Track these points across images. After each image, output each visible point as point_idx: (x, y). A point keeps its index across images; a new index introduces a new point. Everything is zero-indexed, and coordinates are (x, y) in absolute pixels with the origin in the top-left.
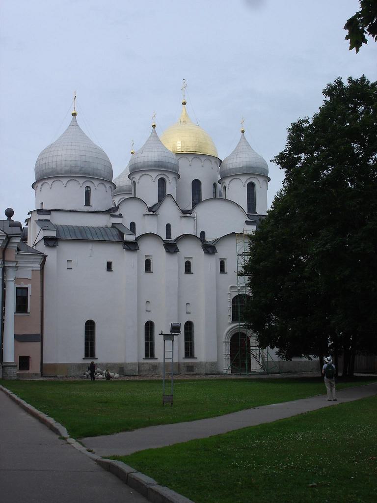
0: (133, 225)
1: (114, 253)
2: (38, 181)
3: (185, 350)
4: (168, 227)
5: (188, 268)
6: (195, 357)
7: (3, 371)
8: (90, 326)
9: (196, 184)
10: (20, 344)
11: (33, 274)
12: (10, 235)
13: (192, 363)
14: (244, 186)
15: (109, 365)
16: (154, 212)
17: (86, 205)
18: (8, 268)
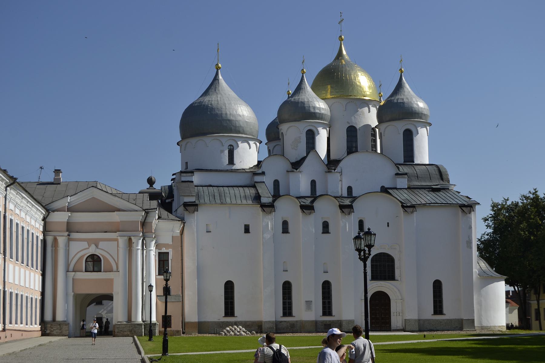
3: (323, 309)
6: (333, 315)
12: (147, 209)
13: (330, 321)
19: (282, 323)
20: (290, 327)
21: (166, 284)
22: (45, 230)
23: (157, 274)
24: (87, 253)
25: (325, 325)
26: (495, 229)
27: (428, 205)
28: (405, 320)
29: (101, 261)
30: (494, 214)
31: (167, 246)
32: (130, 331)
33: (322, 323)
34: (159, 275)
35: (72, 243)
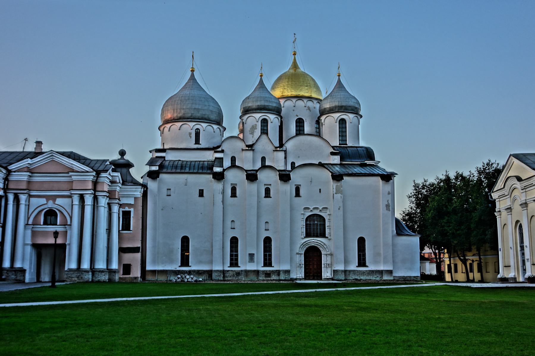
0: (233, 159)
2: (163, 124)
4: (263, 159)
5: (268, 192)
7: (93, 275)
9: (300, 123)
13: (270, 271)
14: (336, 122)
15: (200, 272)
16: (249, 148)
17: (195, 144)
18: (98, 197)
19: (229, 272)
20: (235, 276)
23: (121, 229)
25: (265, 274)
26: (417, 204)
27: (354, 174)
28: (334, 270)
30: (416, 192)
31: (130, 205)
32: (77, 277)
33: (263, 272)
34: (123, 230)
35: (32, 199)
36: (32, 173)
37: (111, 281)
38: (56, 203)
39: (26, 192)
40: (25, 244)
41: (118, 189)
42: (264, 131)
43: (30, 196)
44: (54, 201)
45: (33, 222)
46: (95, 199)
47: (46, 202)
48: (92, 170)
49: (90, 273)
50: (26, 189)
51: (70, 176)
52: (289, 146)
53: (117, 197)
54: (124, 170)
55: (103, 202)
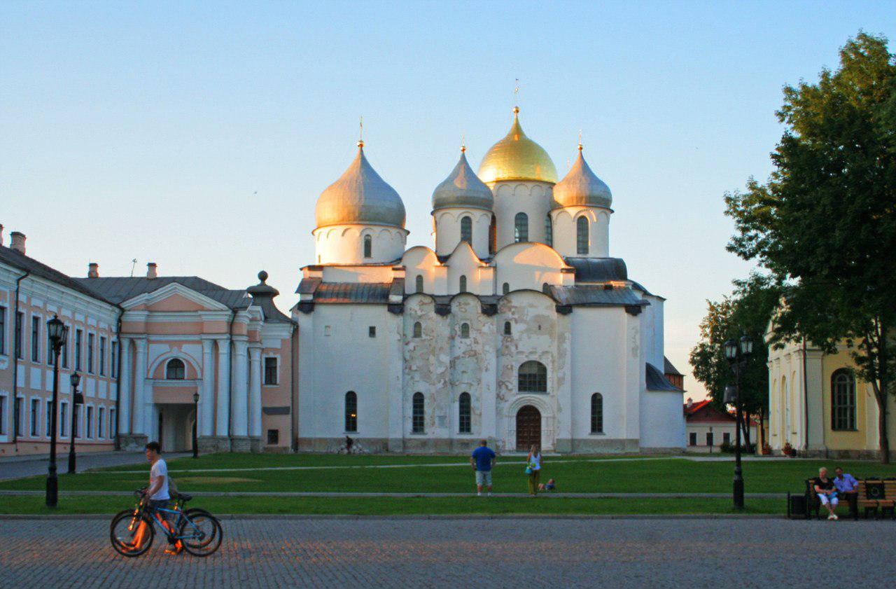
0: (420, 279)
1: (377, 315)
4: (463, 279)
7: (232, 444)
8: (351, 399)
9: (521, 219)
10: (267, 417)
11: (282, 344)
13: (467, 440)
21: (75, 391)
22: (120, 330)
23: (264, 382)
24: (167, 359)
29: (183, 366)
31: (275, 350)
35: (151, 346)
36: (151, 311)
37: (253, 451)
38: (183, 350)
39: (144, 337)
40: (146, 404)
41: (259, 327)
42: (467, 236)
43: (149, 342)
44: (180, 348)
45: (154, 375)
46: (232, 343)
47: (168, 350)
48: (226, 308)
49: (229, 442)
50: (144, 333)
51: (200, 316)
52: (500, 259)
53: (258, 340)
54: (266, 300)
55: (241, 349)
